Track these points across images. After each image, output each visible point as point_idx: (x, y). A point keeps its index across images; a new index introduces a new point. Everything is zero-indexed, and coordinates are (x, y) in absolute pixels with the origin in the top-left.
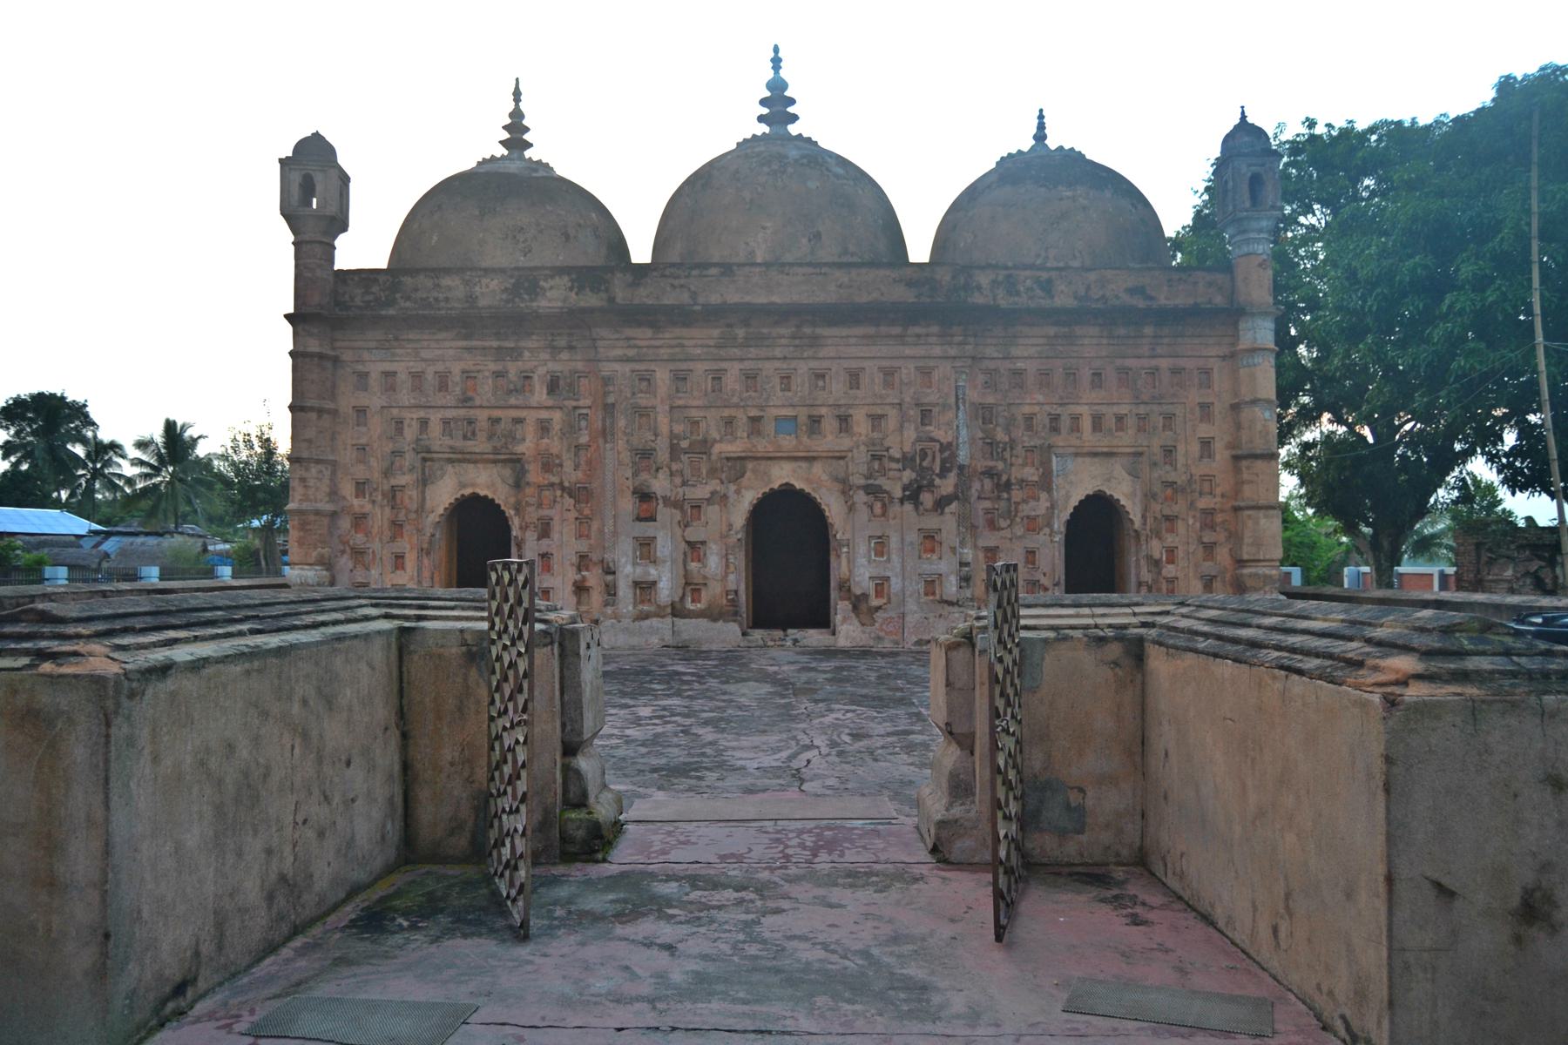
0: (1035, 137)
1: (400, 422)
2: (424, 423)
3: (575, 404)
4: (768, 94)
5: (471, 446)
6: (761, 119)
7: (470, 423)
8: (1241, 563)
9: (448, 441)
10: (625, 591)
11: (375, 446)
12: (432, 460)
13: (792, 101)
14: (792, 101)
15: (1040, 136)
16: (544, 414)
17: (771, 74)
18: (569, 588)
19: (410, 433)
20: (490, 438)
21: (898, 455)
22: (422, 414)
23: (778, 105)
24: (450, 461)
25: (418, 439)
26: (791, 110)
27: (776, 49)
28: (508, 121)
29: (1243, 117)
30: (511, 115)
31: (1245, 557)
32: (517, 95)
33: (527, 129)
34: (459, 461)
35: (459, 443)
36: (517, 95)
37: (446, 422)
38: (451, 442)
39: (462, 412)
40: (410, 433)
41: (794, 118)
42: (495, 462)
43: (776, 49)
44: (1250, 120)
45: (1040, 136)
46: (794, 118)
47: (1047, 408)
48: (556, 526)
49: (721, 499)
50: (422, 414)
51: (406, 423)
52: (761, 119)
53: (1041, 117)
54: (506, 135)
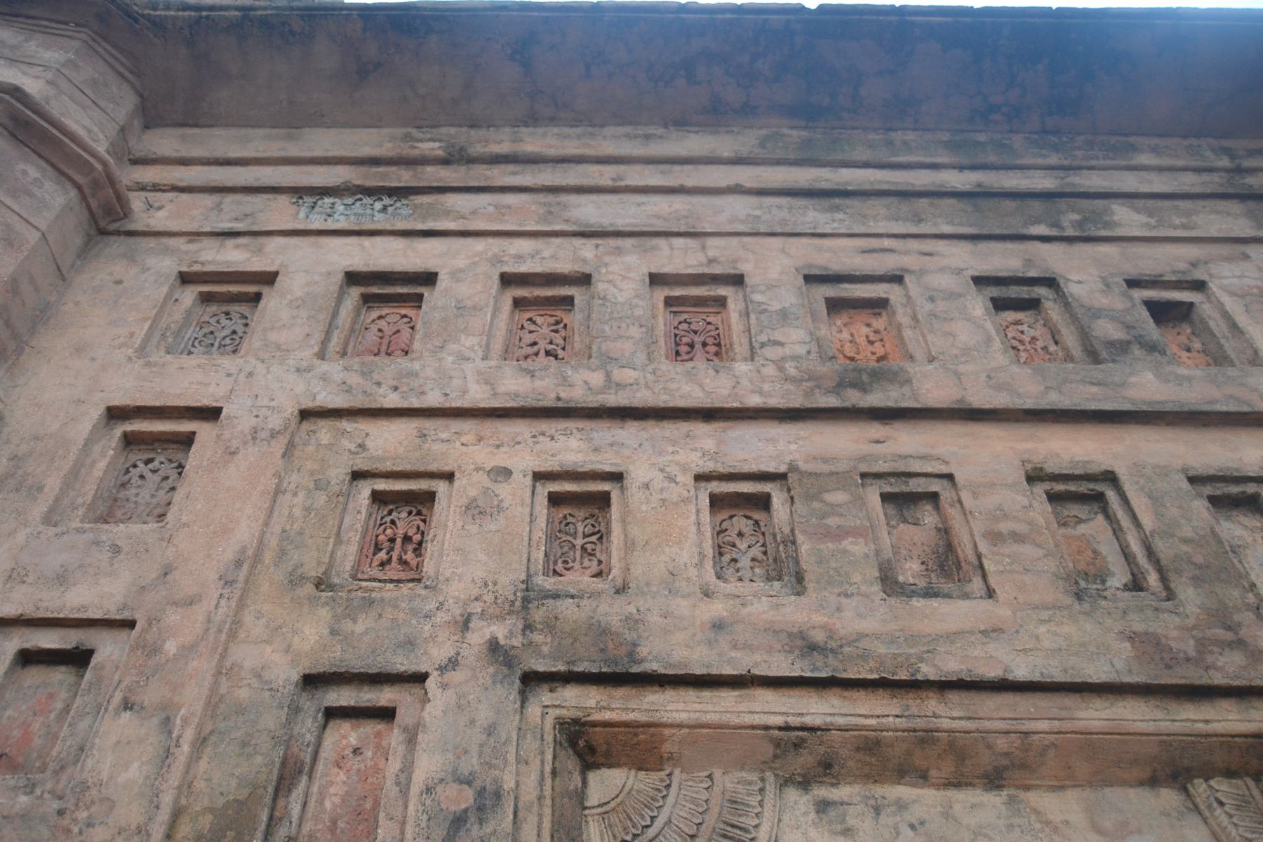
1: (406, 500)
2: (582, 501)
5: (953, 634)
7: (905, 498)
9: (766, 605)
11: (179, 631)
12: (641, 748)
19: (482, 548)
20: (1083, 584)
22: (572, 447)
24: (803, 760)
25: (528, 596)
34: (880, 760)
35: (864, 621)
37: (738, 497)
38: (797, 612)
40: (482, 548)
42: (1175, 768)
50: (572, 447)
51: (468, 486)
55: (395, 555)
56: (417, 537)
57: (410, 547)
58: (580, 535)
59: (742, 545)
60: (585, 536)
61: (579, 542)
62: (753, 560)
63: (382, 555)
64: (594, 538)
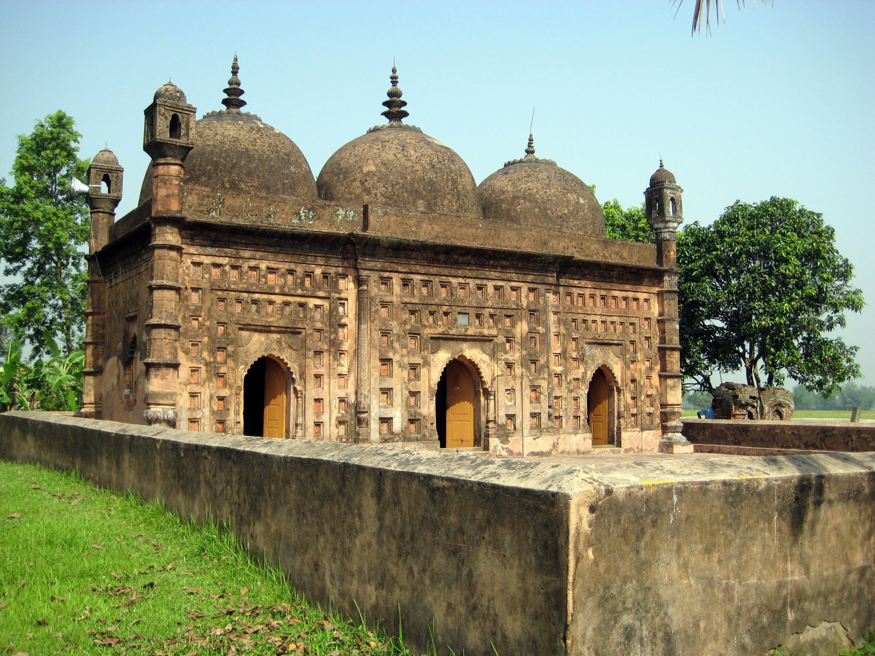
0: (527, 151)
3: (337, 296)
4: (388, 99)
6: (385, 114)
8: (663, 405)
10: (374, 425)
13: (404, 104)
14: (404, 104)
15: (530, 152)
16: (318, 302)
17: (389, 87)
18: (334, 422)
21: (519, 341)
23: (395, 108)
26: (403, 109)
27: (394, 71)
28: (228, 86)
29: (662, 166)
30: (230, 83)
31: (669, 403)
32: (235, 71)
33: (242, 92)
36: (235, 71)
39: (265, 296)
41: (406, 114)
43: (394, 71)
44: (665, 168)
45: (530, 152)
46: (406, 114)
47: (582, 316)
48: (326, 379)
49: (427, 363)
52: (385, 114)
53: (531, 140)
54: (226, 96)
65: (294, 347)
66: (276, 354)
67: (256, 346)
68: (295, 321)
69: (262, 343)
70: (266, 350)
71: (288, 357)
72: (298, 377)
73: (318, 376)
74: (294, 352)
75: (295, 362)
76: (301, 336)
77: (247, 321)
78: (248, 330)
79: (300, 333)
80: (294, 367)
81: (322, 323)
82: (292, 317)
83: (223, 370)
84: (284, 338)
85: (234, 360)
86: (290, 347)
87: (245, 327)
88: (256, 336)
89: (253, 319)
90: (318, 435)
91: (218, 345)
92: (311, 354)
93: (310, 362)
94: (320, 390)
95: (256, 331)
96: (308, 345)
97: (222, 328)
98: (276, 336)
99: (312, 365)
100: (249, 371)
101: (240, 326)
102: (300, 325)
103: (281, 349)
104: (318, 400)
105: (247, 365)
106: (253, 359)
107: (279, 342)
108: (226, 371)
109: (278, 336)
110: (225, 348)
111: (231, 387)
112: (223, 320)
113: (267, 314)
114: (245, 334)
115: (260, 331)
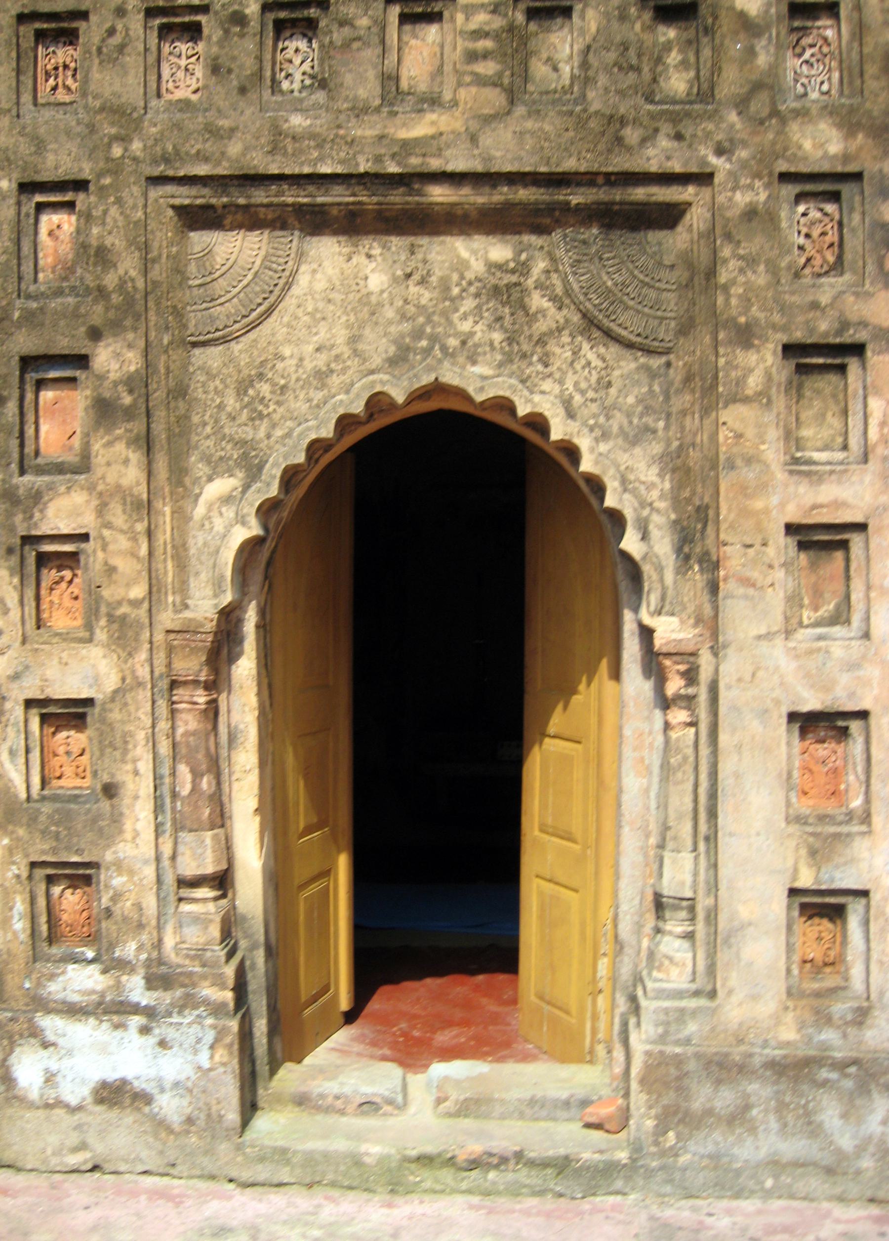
55: (60, 80)
56: (73, 65)
57: (69, 73)
58: (184, 57)
59: (297, 61)
60: (188, 58)
61: (183, 62)
62: (304, 74)
63: (52, 82)
64: (193, 59)
65: (629, 324)
66: (480, 380)
67: (332, 332)
68: (616, 122)
69: (368, 308)
70: (399, 359)
71: (576, 400)
72: (663, 546)
73: (822, 540)
74: (628, 364)
75: (633, 440)
76: (677, 241)
77: (244, 152)
78: (251, 219)
79: (669, 216)
80: (627, 473)
81: (848, 121)
82: (596, 100)
83: (64, 512)
84: (544, 261)
85: (147, 444)
86: (594, 326)
87: (226, 201)
88: (326, 262)
89: (278, 139)
90: (817, 981)
91: (26, 342)
92: (762, 364)
93: (750, 428)
94: (841, 643)
95: (315, 222)
96: (731, 304)
97: (66, 222)
98: (479, 254)
99: (772, 452)
100: (267, 510)
101: (185, 196)
102: (659, 154)
103: (522, 347)
104: (821, 725)
105: (253, 472)
106: (303, 424)
107: (504, 293)
108: (87, 522)
109: (499, 250)
110: (82, 361)
111: (124, 635)
112: (60, 162)
113: (390, 83)
114: (235, 251)
115: (351, 224)
